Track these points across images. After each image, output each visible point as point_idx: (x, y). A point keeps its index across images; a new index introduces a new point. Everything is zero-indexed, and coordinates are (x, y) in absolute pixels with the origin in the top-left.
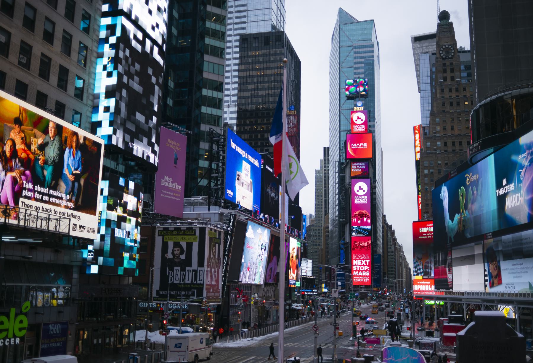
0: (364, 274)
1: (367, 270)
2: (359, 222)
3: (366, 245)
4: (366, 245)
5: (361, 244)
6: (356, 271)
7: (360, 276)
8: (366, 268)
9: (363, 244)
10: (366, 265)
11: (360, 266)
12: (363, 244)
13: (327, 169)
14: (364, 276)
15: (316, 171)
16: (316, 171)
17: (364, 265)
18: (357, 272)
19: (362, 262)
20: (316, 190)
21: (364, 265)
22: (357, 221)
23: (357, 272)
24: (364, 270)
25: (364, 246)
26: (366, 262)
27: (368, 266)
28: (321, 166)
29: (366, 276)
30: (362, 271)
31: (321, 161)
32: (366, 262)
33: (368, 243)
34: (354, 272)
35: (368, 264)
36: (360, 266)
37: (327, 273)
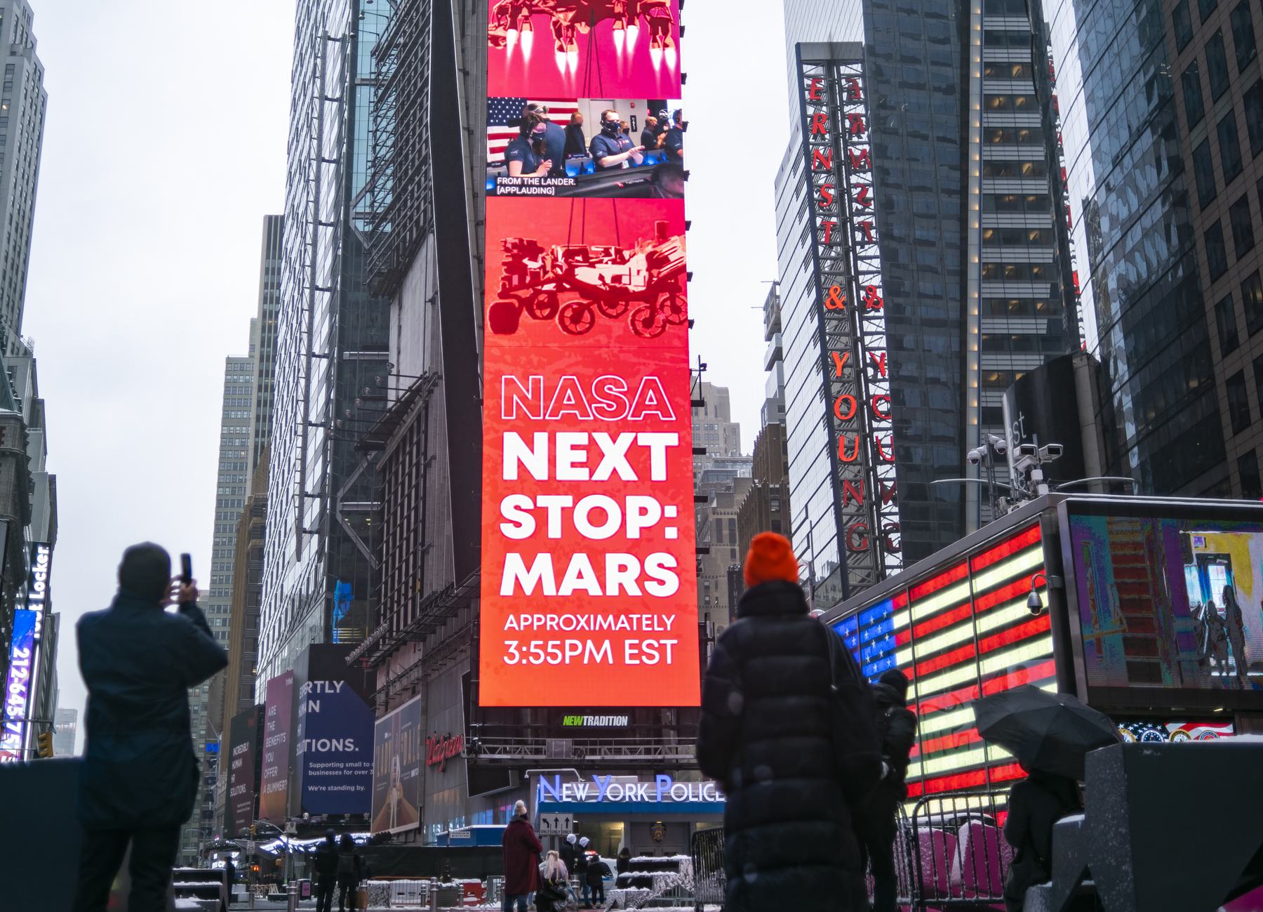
0: (622, 574)
1: (648, 542)
2: (568, 60)
3: (637, 283)
4: (637, 283)
5: (585, 275)
6: (528, 548)
7: (580, 600)
8: (642, 512)
9: (609, 270)
10: (644, 484)
11: (577, 490)
12: (609, 270)
13: (274, 307)
14: (622, 604)
15: (229, 361)
16: (229, 361)
17: (616, 489)
18: (544, 562)
19: (594, 455)
20: (227, 443)
21: (616, 489)
22: (543, 52)
23: (544, 562)
24: (619, 542)
25: (615, 295)
26: (638, 456)
27: (660, 492)
28: (252, 347)
29: (647, 603)
30: (597, 553)
31: (253, 322)
32: (638, 456)
33: (655, 261)
34: (514, 562)
35: (659, 472)
36: (577, 490)
37: (242, 748)
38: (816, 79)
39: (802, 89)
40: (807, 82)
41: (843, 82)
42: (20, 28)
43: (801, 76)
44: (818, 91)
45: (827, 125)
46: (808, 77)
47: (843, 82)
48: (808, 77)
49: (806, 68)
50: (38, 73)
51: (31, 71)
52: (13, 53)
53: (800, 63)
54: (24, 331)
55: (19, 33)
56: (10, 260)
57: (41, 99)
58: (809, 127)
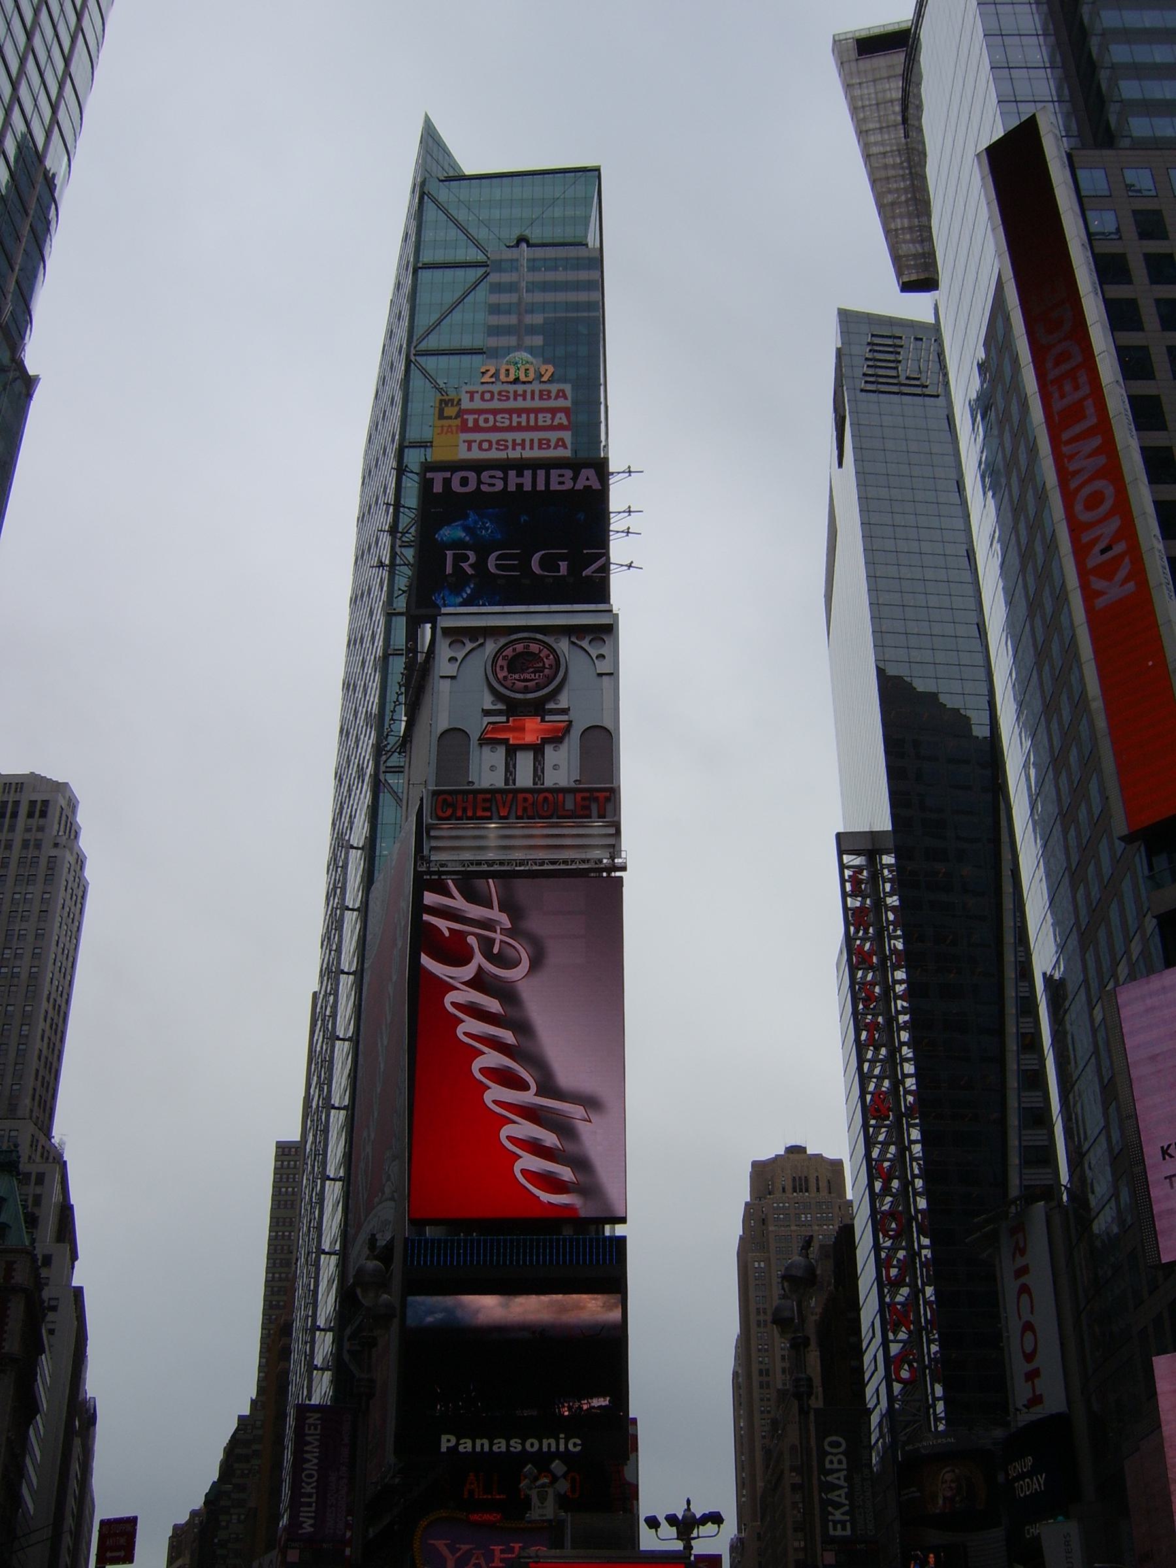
38: (858, 869)
39: (843, 881)
40: (847, 873)
41: (886, 872)
42: (64, 818)
43: (842, 867)
44: (861, 882)
45: (871, 917)
46: (848, 867)
47: (886, 872)
48: (848, 867)
49: (846, 858)
50: (80, 862)
51: (73, 861)
52: (56, 845)
53: (840, 853)
54: (56, 1132)
55: (63, 822)
56: (43, 1059)
57: (82, 888)
58: (853, 918)
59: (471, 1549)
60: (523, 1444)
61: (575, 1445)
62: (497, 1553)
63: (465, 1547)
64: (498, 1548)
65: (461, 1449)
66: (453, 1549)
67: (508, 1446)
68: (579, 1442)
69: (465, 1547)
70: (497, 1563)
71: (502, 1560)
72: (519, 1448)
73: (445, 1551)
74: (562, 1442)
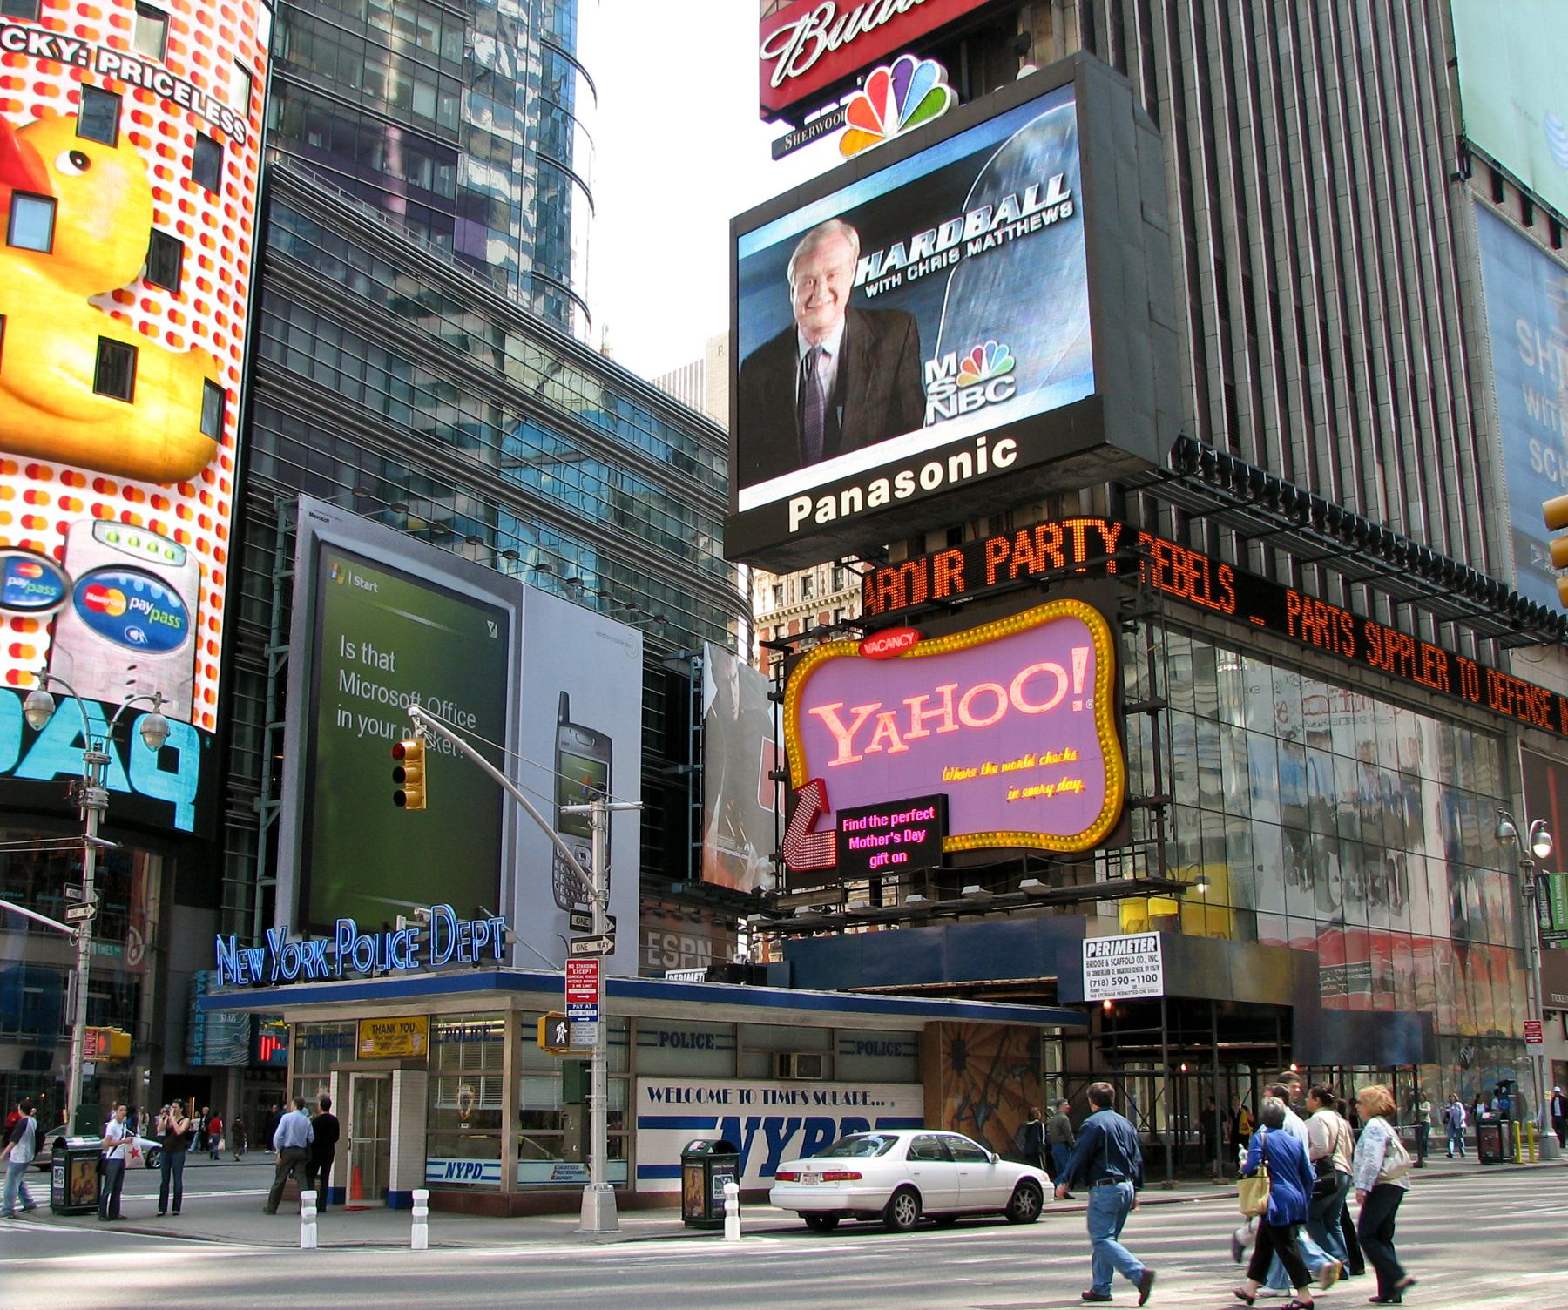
59: (874, 713)
60: (916, 479)
61: (1005, 453)
62: (916, 710)
63: (864, 711)
64: (915, 702)
65: (820, 519)
66: (846, 719)
67: (893, 488)
68: (1009, 443)
69: (864, 711)
70: (917, 731)
71: (925, 723)
72: (911, 487)
73: (835, 725)
74: (982, 454)
